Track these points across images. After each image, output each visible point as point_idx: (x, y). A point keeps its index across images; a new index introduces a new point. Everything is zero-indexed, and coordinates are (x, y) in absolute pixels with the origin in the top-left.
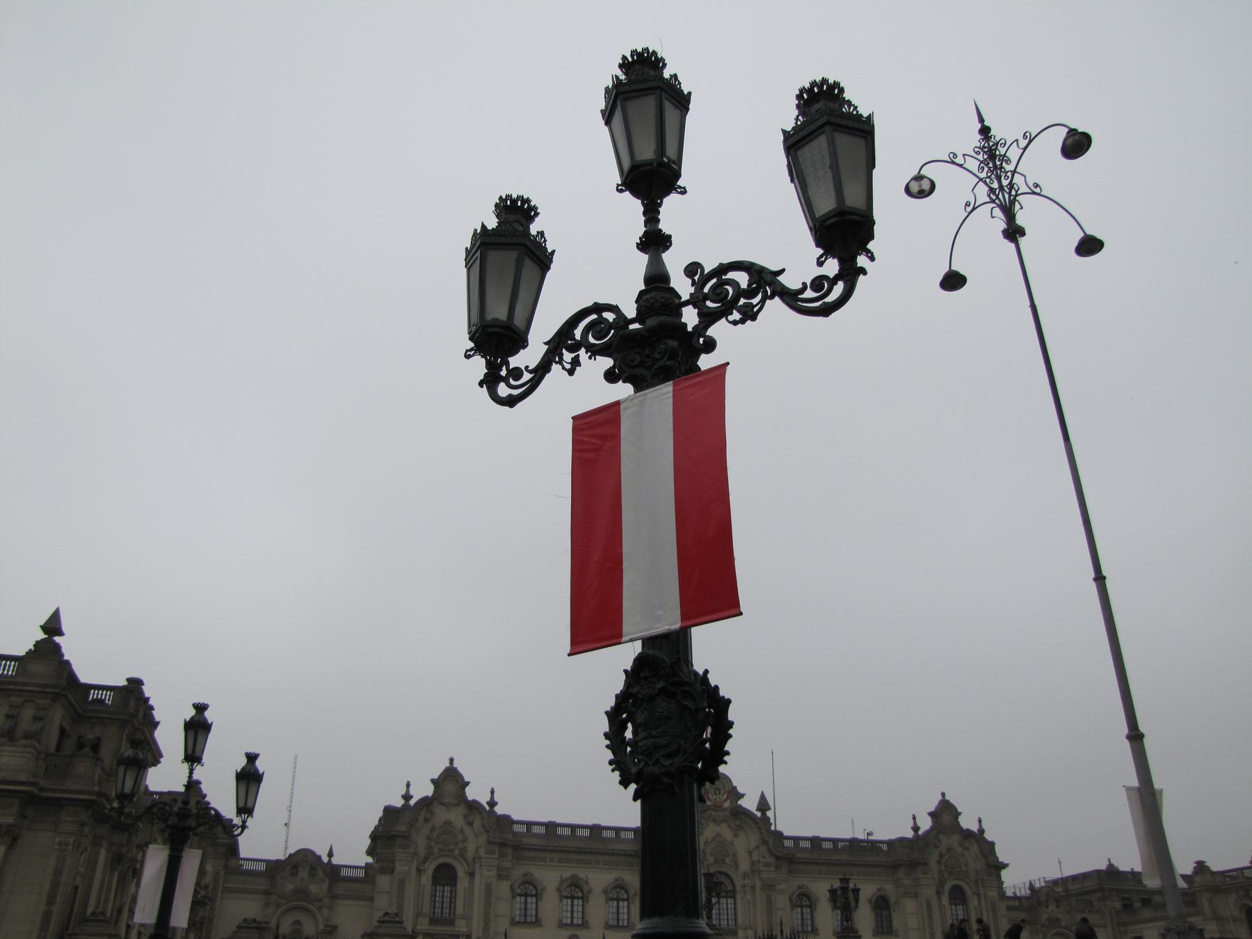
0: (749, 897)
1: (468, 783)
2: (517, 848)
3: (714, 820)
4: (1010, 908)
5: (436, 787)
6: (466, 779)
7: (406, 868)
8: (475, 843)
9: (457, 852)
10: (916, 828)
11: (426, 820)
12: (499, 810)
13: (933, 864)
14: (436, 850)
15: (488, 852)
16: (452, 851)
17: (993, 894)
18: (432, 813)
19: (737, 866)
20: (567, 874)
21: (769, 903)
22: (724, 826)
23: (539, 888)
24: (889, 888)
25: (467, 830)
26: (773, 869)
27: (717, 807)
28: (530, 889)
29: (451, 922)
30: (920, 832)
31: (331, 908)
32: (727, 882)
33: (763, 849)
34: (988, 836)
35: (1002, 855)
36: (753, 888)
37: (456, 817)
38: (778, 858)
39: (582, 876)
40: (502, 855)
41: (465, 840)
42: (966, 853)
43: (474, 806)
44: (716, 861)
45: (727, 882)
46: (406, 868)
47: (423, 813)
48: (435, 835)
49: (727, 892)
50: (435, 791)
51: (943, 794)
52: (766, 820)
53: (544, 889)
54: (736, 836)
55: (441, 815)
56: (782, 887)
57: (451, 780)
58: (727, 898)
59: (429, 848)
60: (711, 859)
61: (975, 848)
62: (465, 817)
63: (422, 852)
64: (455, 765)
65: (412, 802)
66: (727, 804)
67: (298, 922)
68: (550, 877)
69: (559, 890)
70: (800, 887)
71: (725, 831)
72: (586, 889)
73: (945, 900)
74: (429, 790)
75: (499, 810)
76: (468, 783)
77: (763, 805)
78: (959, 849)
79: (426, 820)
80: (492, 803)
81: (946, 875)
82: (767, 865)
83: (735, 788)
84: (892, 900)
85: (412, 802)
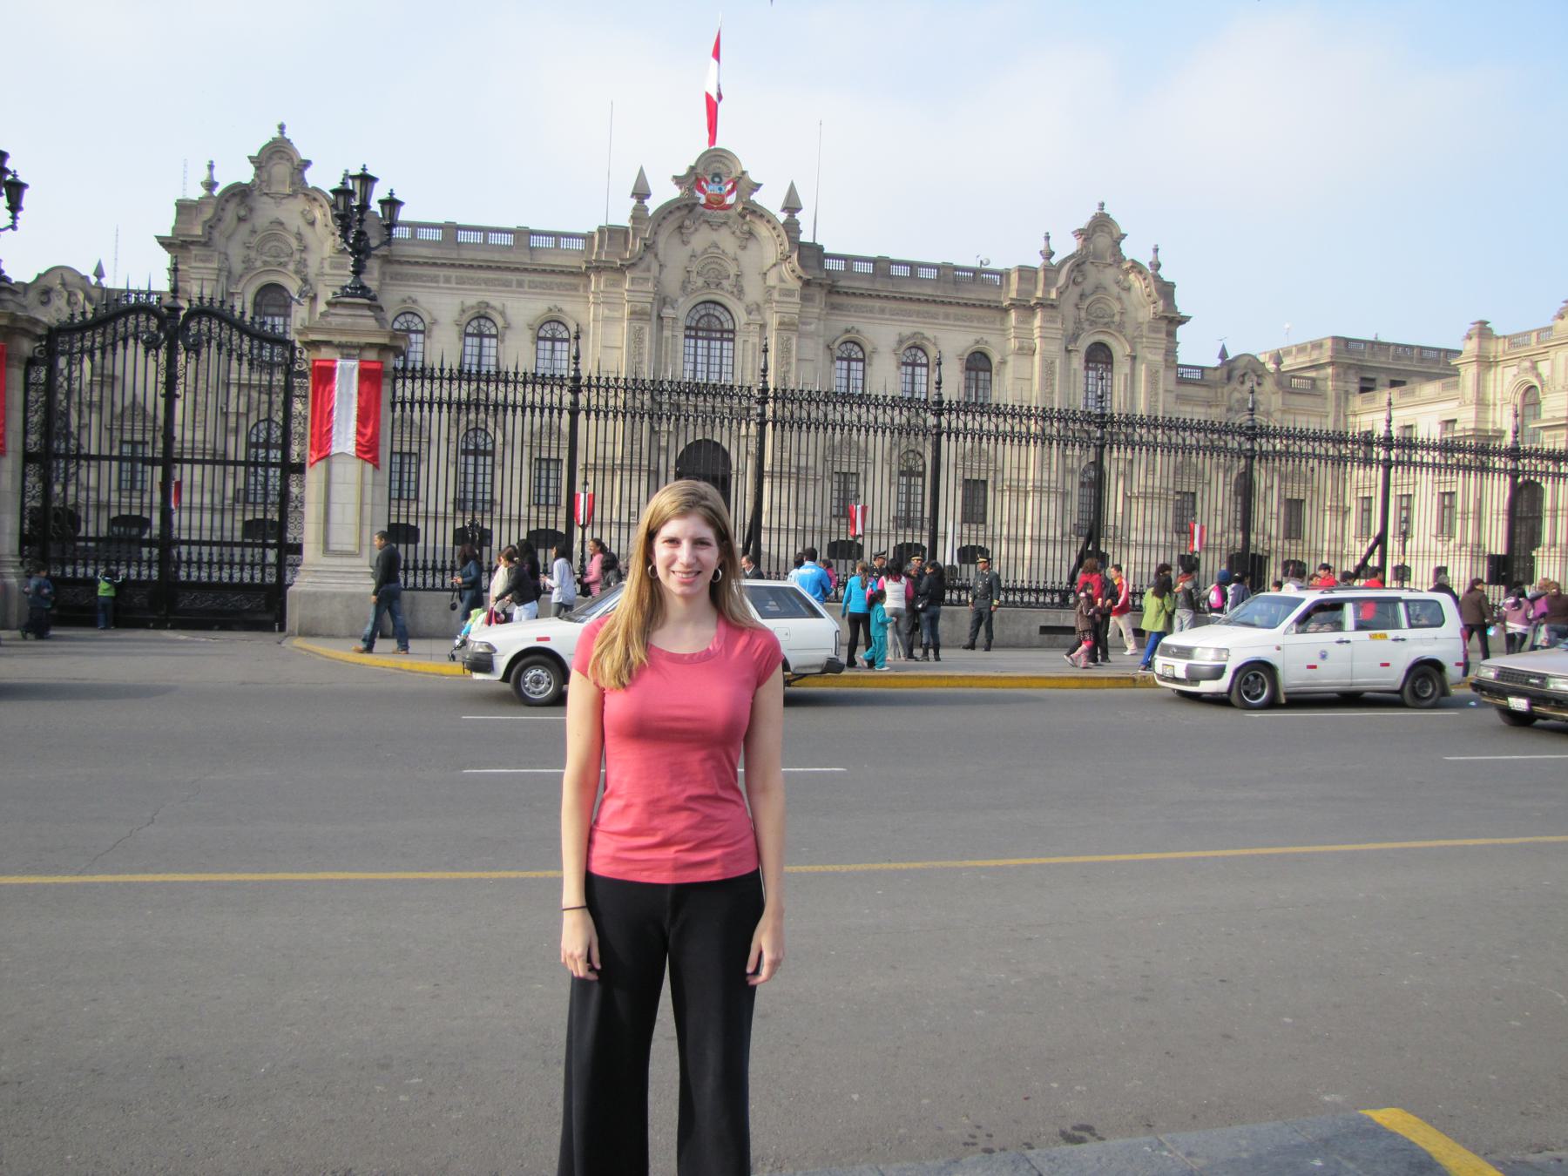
1: (307, 164)
4: (1181, 381)
5: (257, 168)
6: (304, 157)
9: (291, 267)
10: (1049, 254)
11: (241, 219)
13: (1068, 309)
14: (258, 264)
15: (334, 266)
16: (284, 265)
17: (1158, 358)
18: (251, 210)
19: (741, 291)
20: (472, 300)
22: (725, 232)
23: (427, 320)
25: (306, 230)
26: (797, 299)
30: (1054, 260)
32: (724, 317)
34: (1166, 274)
35: (1182, 305)
36: (763, 326)
37: (291, 213)
39: (495, 303)
41: (304, 249)
44: (708, 284)
45: (724, 317)
48: (255, 240)
49: (722, 331)
50: (256, 175)
51: (1102, 205)
52: (792, 228)
53: (435, 322)
54: (744, 248)
55: (267, 212)
58: (722, 340)
60: (700, 282)
63: (238, 267)
64: (287, 136)
65: (216, 193)
70: (848, 331)
72: (500, 323)
73: (1078, 362)
74: (246, 175)
76: (307, 164)
78: (1115, 290)
81: (1086, 326)
82: (788, 293)
83: (744, 173)
84: (995, 360)
85: (216, 193)
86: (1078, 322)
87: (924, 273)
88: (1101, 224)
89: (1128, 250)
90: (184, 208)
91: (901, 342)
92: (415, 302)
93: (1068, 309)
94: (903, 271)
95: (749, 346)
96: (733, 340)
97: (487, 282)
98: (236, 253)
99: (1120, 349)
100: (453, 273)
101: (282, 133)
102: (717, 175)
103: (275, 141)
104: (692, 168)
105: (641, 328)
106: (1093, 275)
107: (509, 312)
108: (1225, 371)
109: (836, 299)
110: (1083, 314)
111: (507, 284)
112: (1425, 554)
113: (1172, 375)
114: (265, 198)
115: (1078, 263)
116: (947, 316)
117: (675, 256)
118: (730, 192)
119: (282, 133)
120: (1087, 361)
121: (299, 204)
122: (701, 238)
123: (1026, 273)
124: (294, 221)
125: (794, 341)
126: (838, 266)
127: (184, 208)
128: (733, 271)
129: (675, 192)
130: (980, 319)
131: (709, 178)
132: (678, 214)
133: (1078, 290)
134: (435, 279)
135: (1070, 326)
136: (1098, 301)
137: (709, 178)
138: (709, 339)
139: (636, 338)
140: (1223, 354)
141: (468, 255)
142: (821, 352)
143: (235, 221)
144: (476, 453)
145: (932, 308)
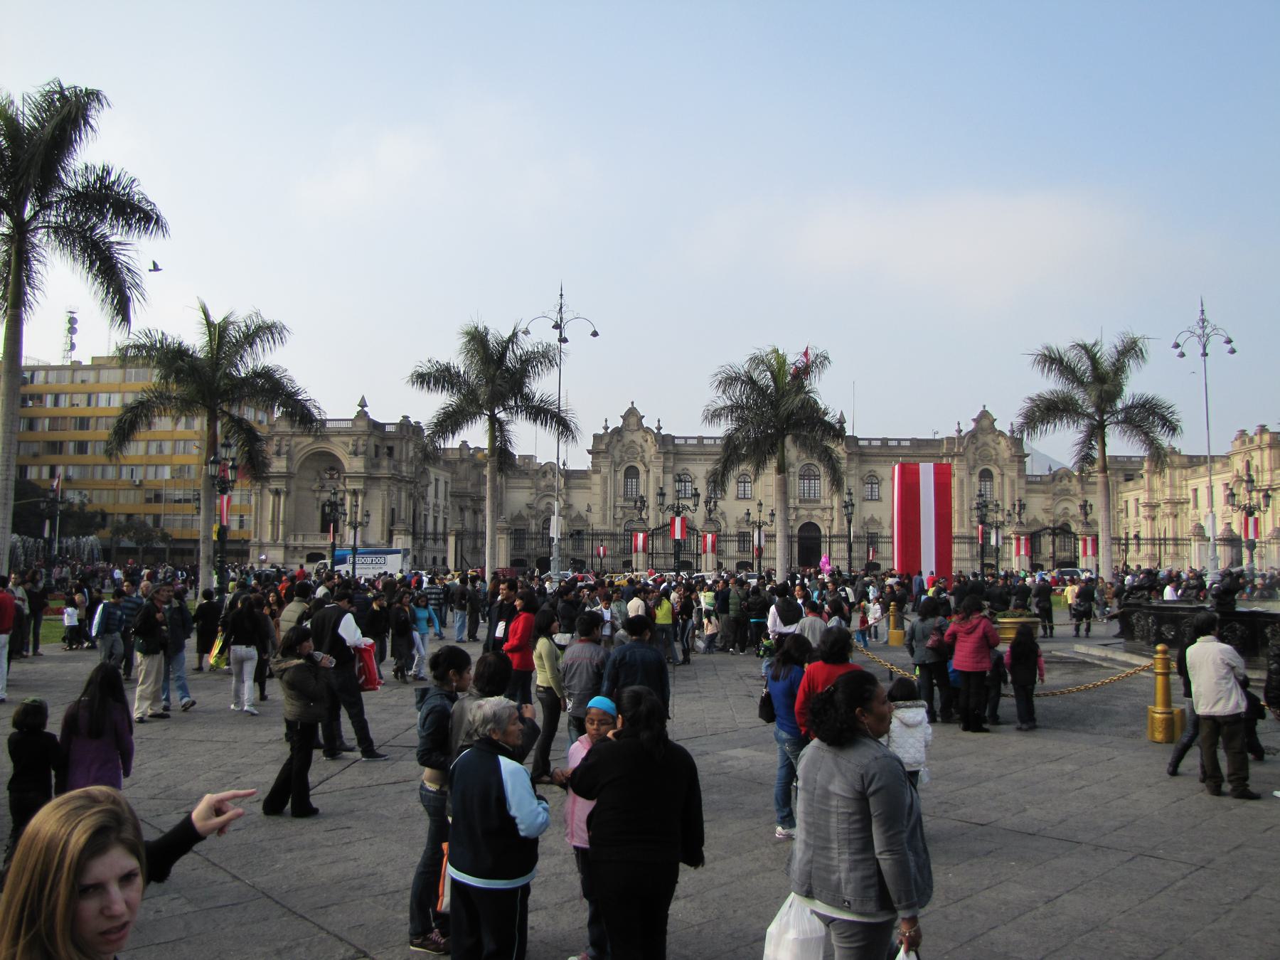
4: (1028, 483)
12: (663, 432)
13: (970, 456)
31: (567, 495)
37: (638, 437)
40: (666, 459)
43: (648, 430)
47: (615, 438)
55: (628, 437)
57: (632, 415)
61: (1003, 442)
63: (618, 460)
73: (975, 479)
74: (620, 423)
78: (992, 444)
80: (659, 428)
86: (975, 460)
87: (903, 443)
88: (984, 414)
90: (596, 437)
93: (970, 456)
94: (895, 443)
99: (995, 471)
106: (981, 439)
108: (1050, 478)
112: (1133, 559)
113: (1023, 481)
115: (973, 435)
121: (641, 433)
123: (950, 440)
124: (639, 440)
126: (865, 443)
127: (596, 437)
135: (972, 463)
140: (1050, 469)
141: (708, 449)
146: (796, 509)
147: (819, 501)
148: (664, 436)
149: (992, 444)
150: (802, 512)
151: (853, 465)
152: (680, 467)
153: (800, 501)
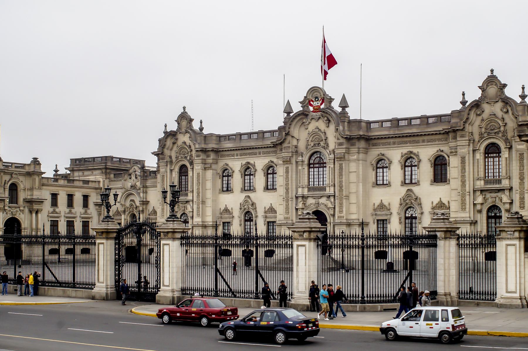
0: (332, 166)
2: (216, 151)
3: (312, 118)
7: (164, 170)
8: (194, 153)
9: (188, 158)
11: (174, 143)
12: (205, 132)
16: (186, 157)
18: (177, 139)
19: (328, 145)
20: (244, 163)
21: (341, 168)
22: (320, 121)
24: (446, 149)
27: (317, 110)
28: (226, 174)
29: (187, 195)
33: (338, 134)
36: (334, 160)
38: (349, 139)
39: (252, 162)
41: (191, 150)
42: (506, 116)
46: (164, 170)
51: (492, 71)
52: (344, 114)
54: (328, 127)
56: (355, 157)
58: (323, 167)
59: (177, 158)
62: (190, 137)
66: (322, 106)
67: (131, 200)
68: (236, 165)
69: (240, 171)
71: (321, 124)
73: (480, 156)
75: (205, 132)
77: (344, 104)
78: (500, 114)
79: (174, 143)
80: (201, 129)
81: (485, 135)
82: (340, 144)
86: (481, 134)
87: (414, 122)
88: (492, 80)
89: (508, 92)
91: (402, 156)
92: (227, 165)
95: (331, 169)
96: (326, 167)
97: (250, 154)
98: (174, 155)
100: (239, 152)
101: (184, 110)
102: (316, 98)
103: (182, 113)
104: (305, 97)
105: (288, 167)
106: (487, 109)
107: (256, 165)
109: (371, 142)
110: (483, 130)
111: (255, 154)
114: (180, 134)
115: (476, 105)
116: (423, 141)
117: (301, 136)
118: (321, 104)
119: (184, 110)
120: (485, 153)
122: (312, 126)
125: (344, 165)
128: (323, 138)
129: (302, 109)
130: (439, 140)
131: (314, 100)
132: (298, 118)
133: (480, 118)
134: (233, 156)
136: (491, 121)
137: (314, 100)
138: (318, 167)
139: (287, 172)
142: (361, 168)
143: (171, 144)
144: (250, 220)
145: (416, 139)
146: (303, 197)
147: (324, 189)
148: (206, 137)
149: (500, 114)
150: (311, 201)
151: (354, 150)
152: (221, 164)
153: (309, 189)
